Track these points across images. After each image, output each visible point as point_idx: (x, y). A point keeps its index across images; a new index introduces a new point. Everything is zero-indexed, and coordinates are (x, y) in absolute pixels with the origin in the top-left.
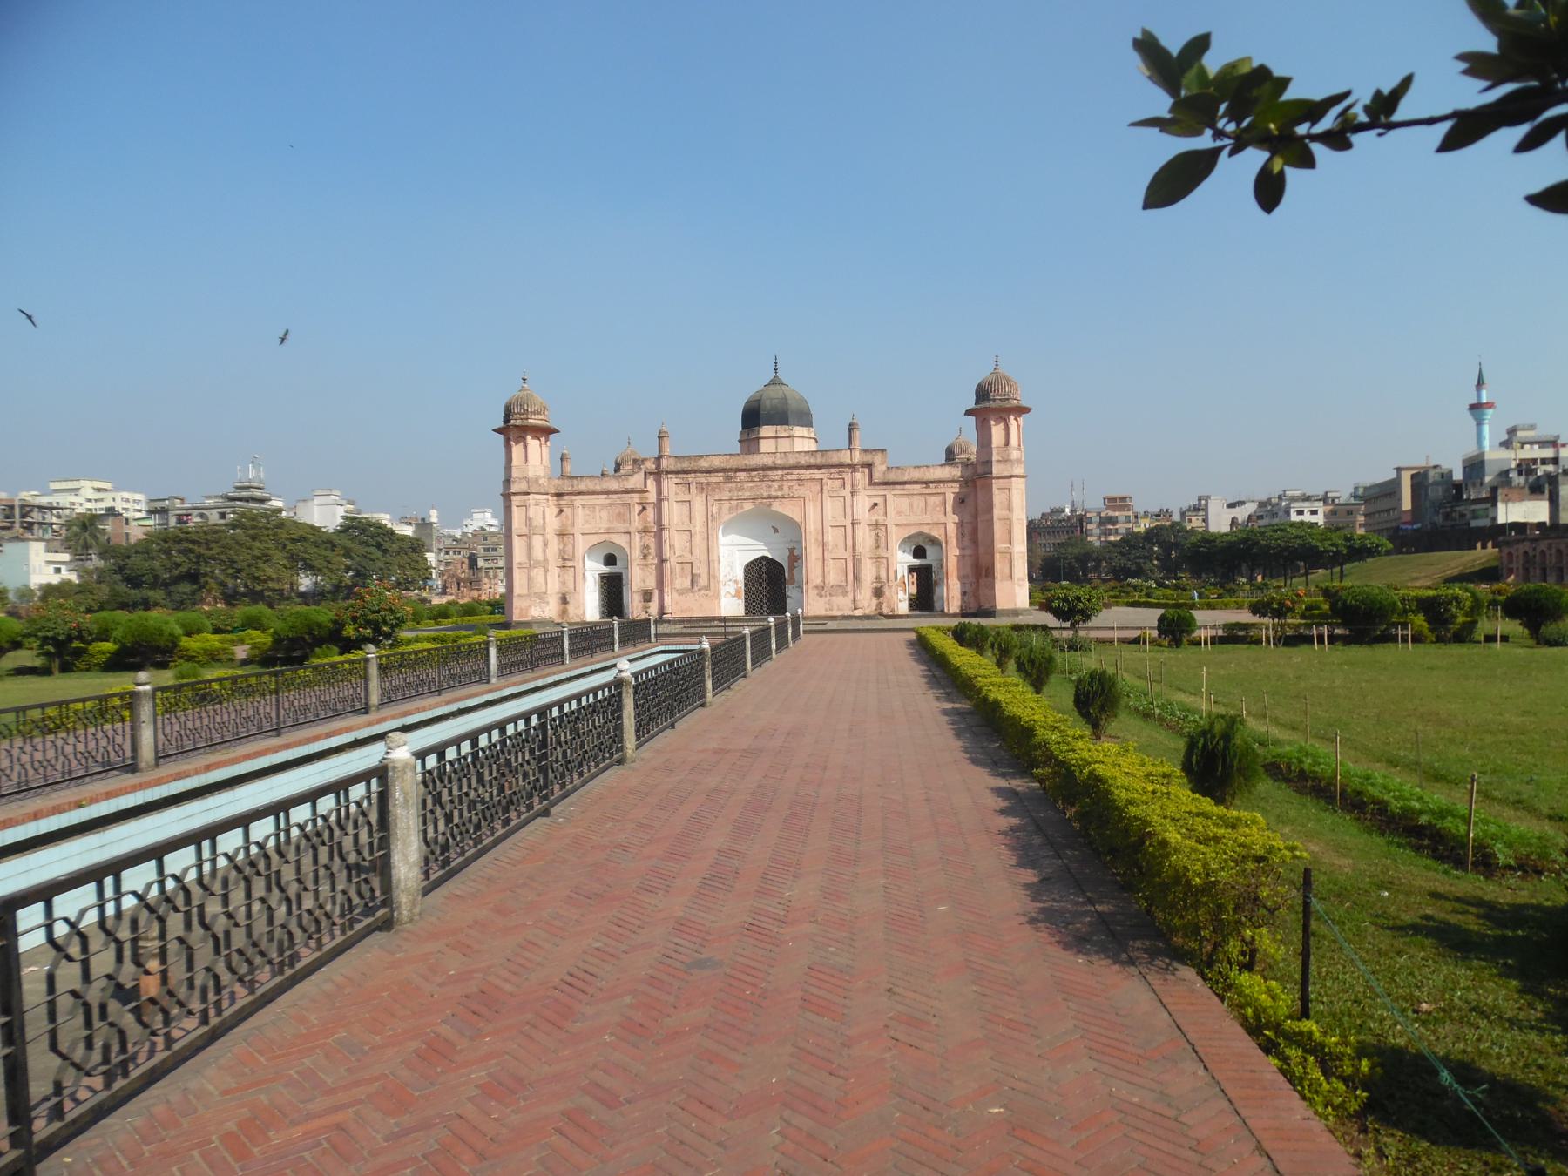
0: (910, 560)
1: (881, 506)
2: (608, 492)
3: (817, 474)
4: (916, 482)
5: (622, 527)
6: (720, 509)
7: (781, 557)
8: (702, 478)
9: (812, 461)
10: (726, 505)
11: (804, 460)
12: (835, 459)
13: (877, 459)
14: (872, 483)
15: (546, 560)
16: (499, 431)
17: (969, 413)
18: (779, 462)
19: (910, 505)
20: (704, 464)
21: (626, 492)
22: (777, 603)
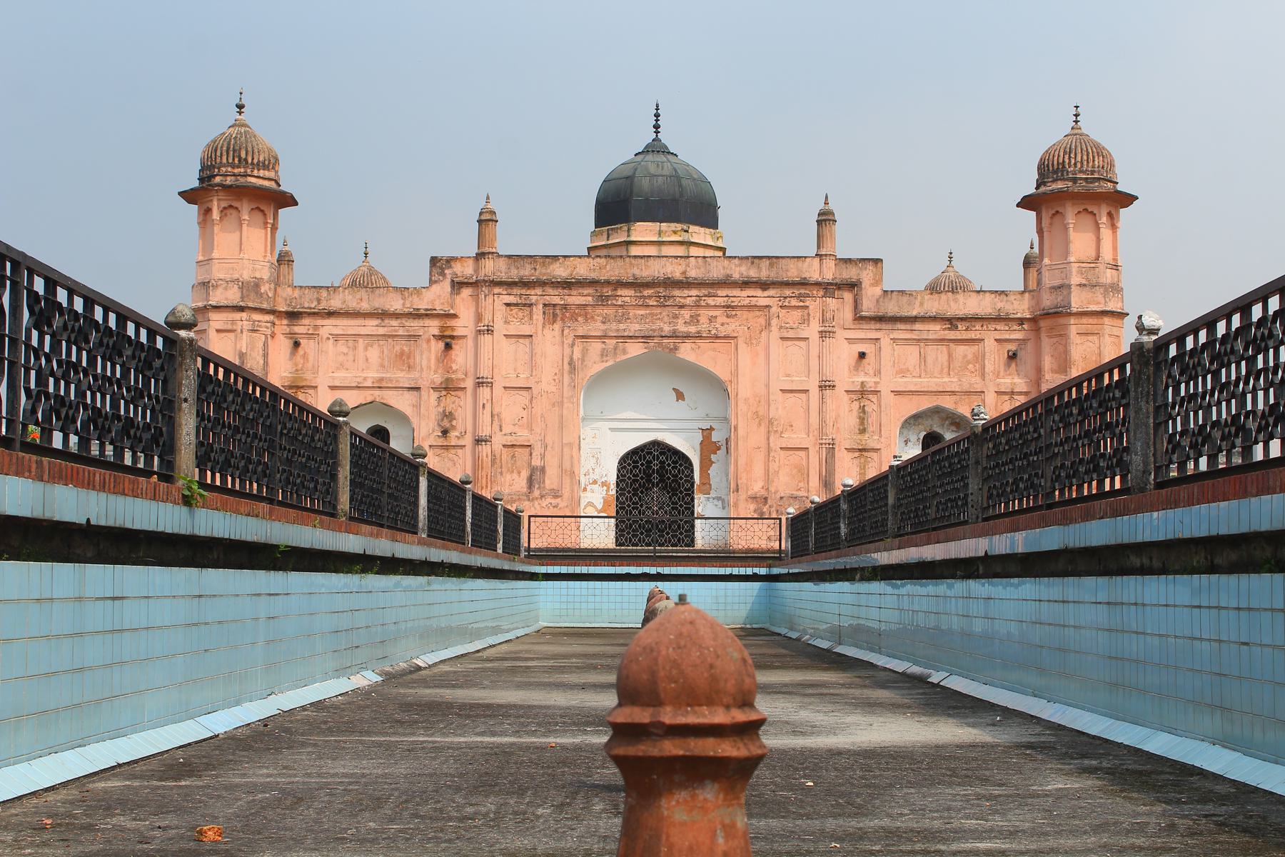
1: (870, 358)
2: (383, 315)
3: (761, 297)
4: (934, 319)
5: (403, 378)
6: (585, 352)
9: (753, 273)
10: (596, 347)
11: (738, 271)
12: (792, 272)
13: (866, 276)
14: (859, 318)
17: (1027, 203)
18: (693, 273)
19: (923, 358)
20: (559, 271)
21: (416, 315)
22: (679, 526)
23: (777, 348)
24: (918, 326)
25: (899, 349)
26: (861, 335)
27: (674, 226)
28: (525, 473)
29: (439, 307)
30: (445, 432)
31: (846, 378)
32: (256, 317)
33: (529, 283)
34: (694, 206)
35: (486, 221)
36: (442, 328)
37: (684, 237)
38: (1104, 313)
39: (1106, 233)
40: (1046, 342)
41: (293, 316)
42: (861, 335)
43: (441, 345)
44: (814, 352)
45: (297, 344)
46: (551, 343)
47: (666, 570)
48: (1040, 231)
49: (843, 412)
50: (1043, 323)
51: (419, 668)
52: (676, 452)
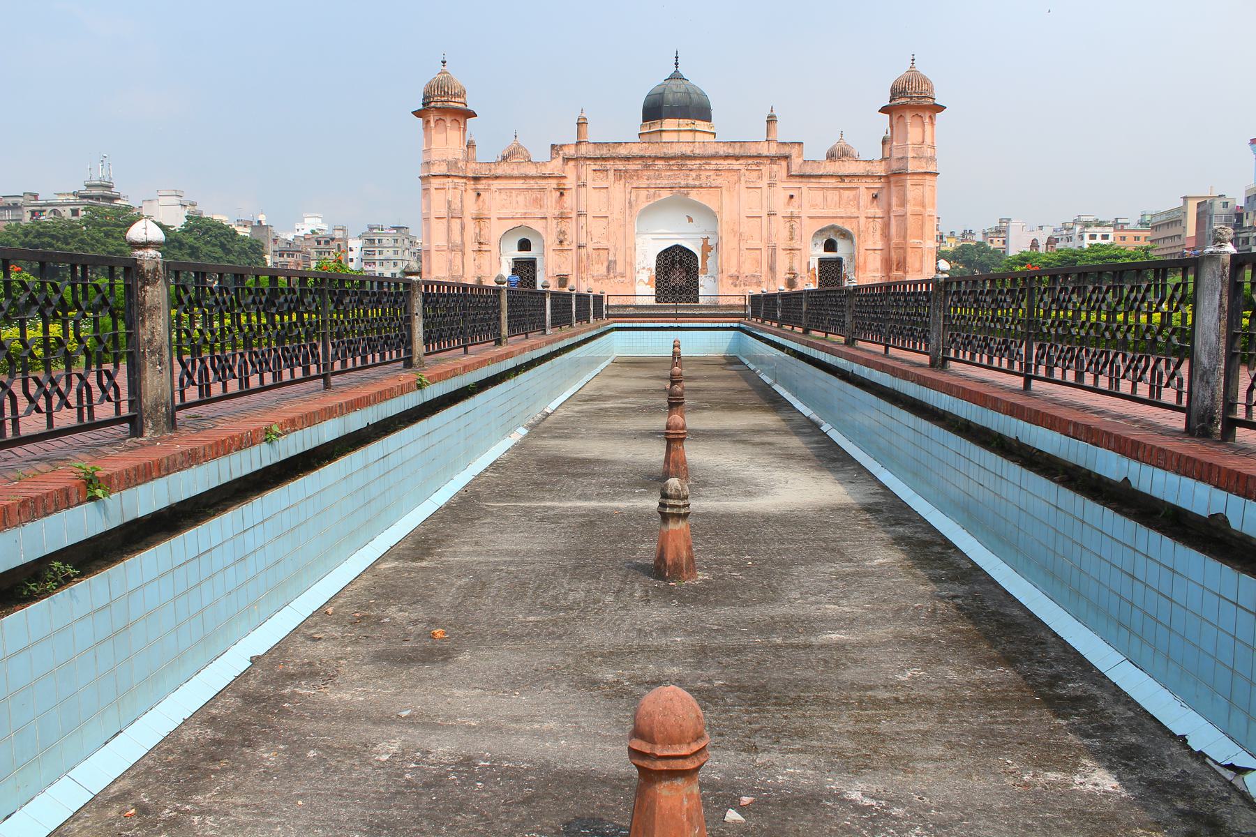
0: (821, 252)
2: (526, 177)
3: (735, 164)
4: (832, 176)
5: (538, 212)
7: (694, 247)
8: (620, 165)
9: (731, 151)
10: (643, 193)
11: (722, 150)
12: (753, 150)
13: (794, 152)
14: (790, 176)
15: (463, 243)
16: (417, 114)
17: (884, 110)
18: (697, 151)
19: (825, 198)
20: (623, 151)
21: (544, 177)
22: (689, 291)
23: (744, 193)
24: (823, 180)
25: (812, 193)
26: (791, 185)
27: (687, 121)
28: (605, 264)
29: (556, 173)
30: (561, 242)
31: (782, 209)
32: (456, 180)
33: (607, 158)
34: (698, 110)
35: (581, 123)
36: (559, 184)
37: (693, 127)
38: (926, 173)
39: (928, 127)
40: (893, 189)
41: (476, 179)
42: (791, 185)
43: (558, 193)
44: (765, 195)
45: (479, 195)
46: (618, 191)
47: (683, 325)
48: (891, 126)
49: (780, 230)
50: (892, 179)
51: (548, 415)
52: (689, 251)
